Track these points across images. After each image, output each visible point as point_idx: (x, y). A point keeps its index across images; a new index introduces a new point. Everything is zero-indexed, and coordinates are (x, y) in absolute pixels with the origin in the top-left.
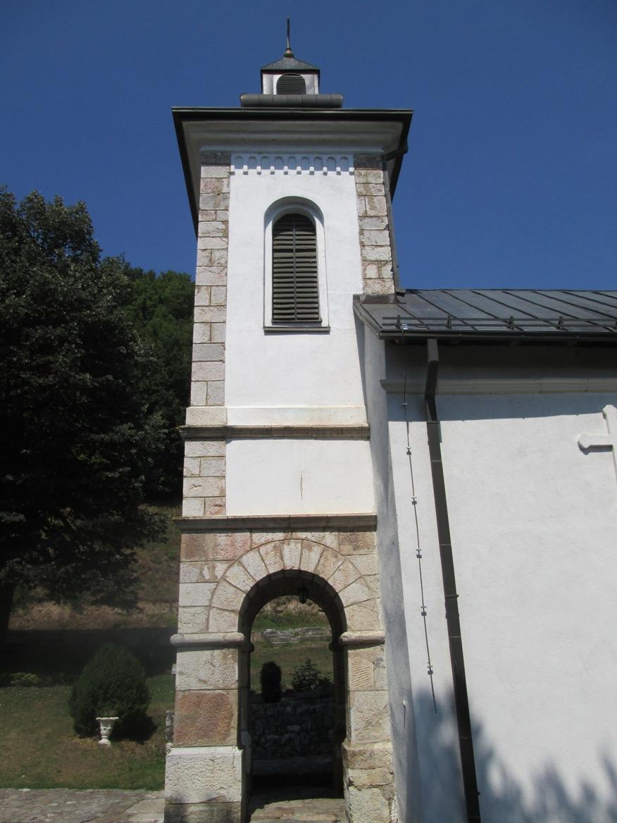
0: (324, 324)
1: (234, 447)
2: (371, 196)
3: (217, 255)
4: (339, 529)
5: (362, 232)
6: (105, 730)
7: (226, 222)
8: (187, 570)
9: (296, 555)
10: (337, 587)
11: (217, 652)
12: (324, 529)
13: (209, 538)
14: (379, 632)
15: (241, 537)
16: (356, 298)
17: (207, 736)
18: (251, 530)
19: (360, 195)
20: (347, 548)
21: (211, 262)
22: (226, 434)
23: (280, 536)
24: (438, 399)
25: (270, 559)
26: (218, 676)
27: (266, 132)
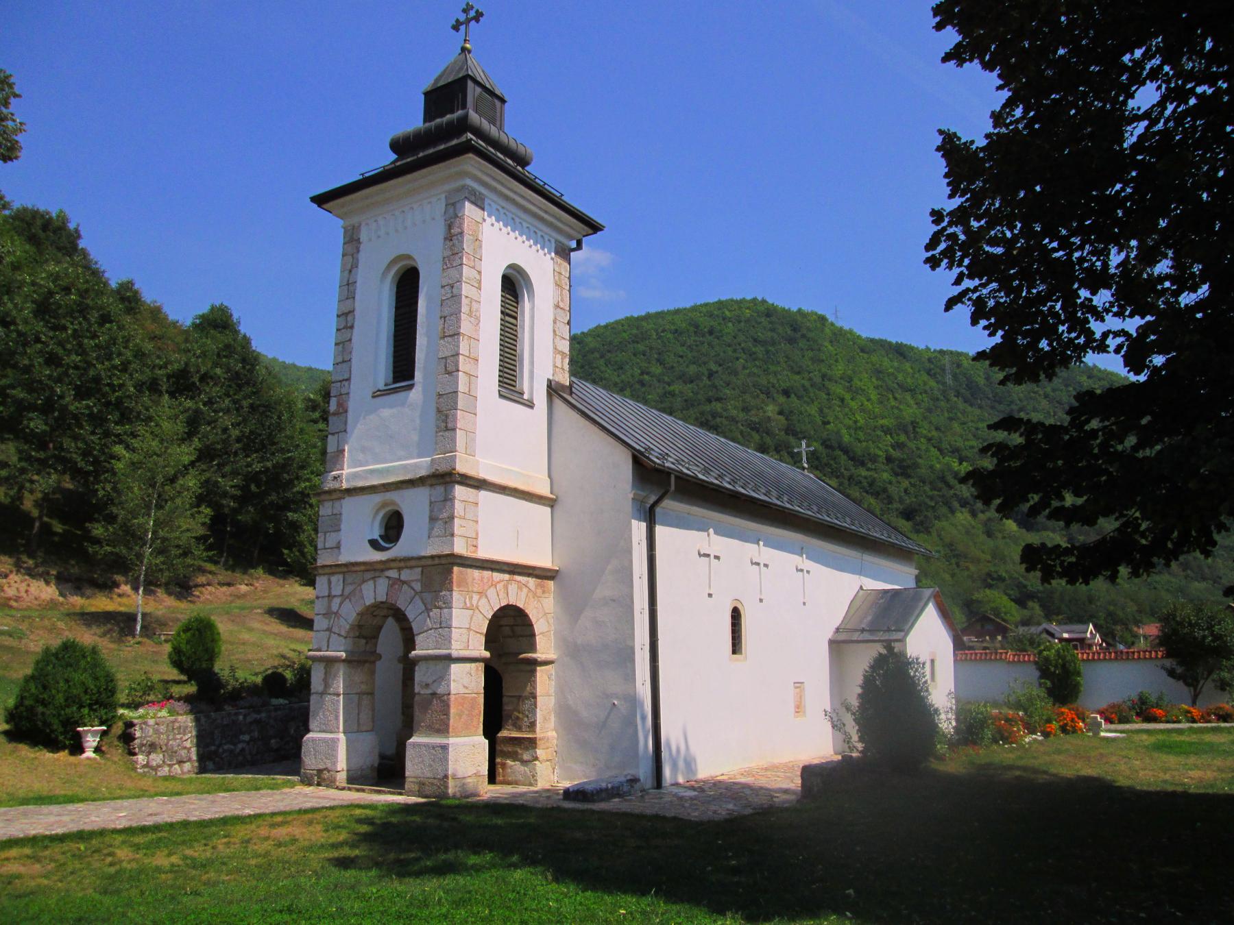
0: (526, 397)
1: (483, 494)
2: (563, 289)
3: (475, 305)
4: (538, 577)
5: (555, 322)
6: (91, 741)
7: (480, 272)
8: (457, 597)
9: (518, 593)
10: (534, 621)
11: (473, 665)
12: (529, 575)
13: (469, 570)
14: (551, 656)
15: (487, 573)
16: (549, 381)
17: (467, 731)
18: (492, 570)
19: (557, 285)
20: (539, 591)
21: (470, 315)
22: (480, 484)
23: (507, 576)
24: (658, 510)
25: (502, 595)
26: (473, 684)
27: (515, 193)
